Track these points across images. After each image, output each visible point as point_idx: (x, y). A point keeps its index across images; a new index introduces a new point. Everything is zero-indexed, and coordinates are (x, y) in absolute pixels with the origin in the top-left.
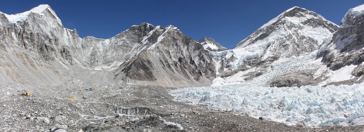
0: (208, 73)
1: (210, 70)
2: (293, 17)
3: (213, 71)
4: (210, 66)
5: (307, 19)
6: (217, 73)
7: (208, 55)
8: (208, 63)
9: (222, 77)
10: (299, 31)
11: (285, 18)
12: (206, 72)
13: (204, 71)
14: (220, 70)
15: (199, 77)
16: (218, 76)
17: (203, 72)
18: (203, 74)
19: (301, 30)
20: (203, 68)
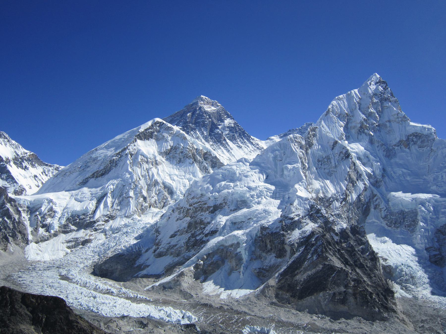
0: (17, 238)
1: (20, 232)
2: (148, 139)
3: (24, 235)
4: (19, 227)
5: (170, 146)
6: (30, 237)
7: (15, 206)
8: (16, 222)
9: (37, 243)
10: (154, 170)
11: (136, 144)
12: (14, 236)
13: (11, 234)
14: (34, 231)
15: (7, 246)
16: (32, 242)
17: (9, 236)
18: (10, 239)
19: (156, 168)
20: (10, 229)
